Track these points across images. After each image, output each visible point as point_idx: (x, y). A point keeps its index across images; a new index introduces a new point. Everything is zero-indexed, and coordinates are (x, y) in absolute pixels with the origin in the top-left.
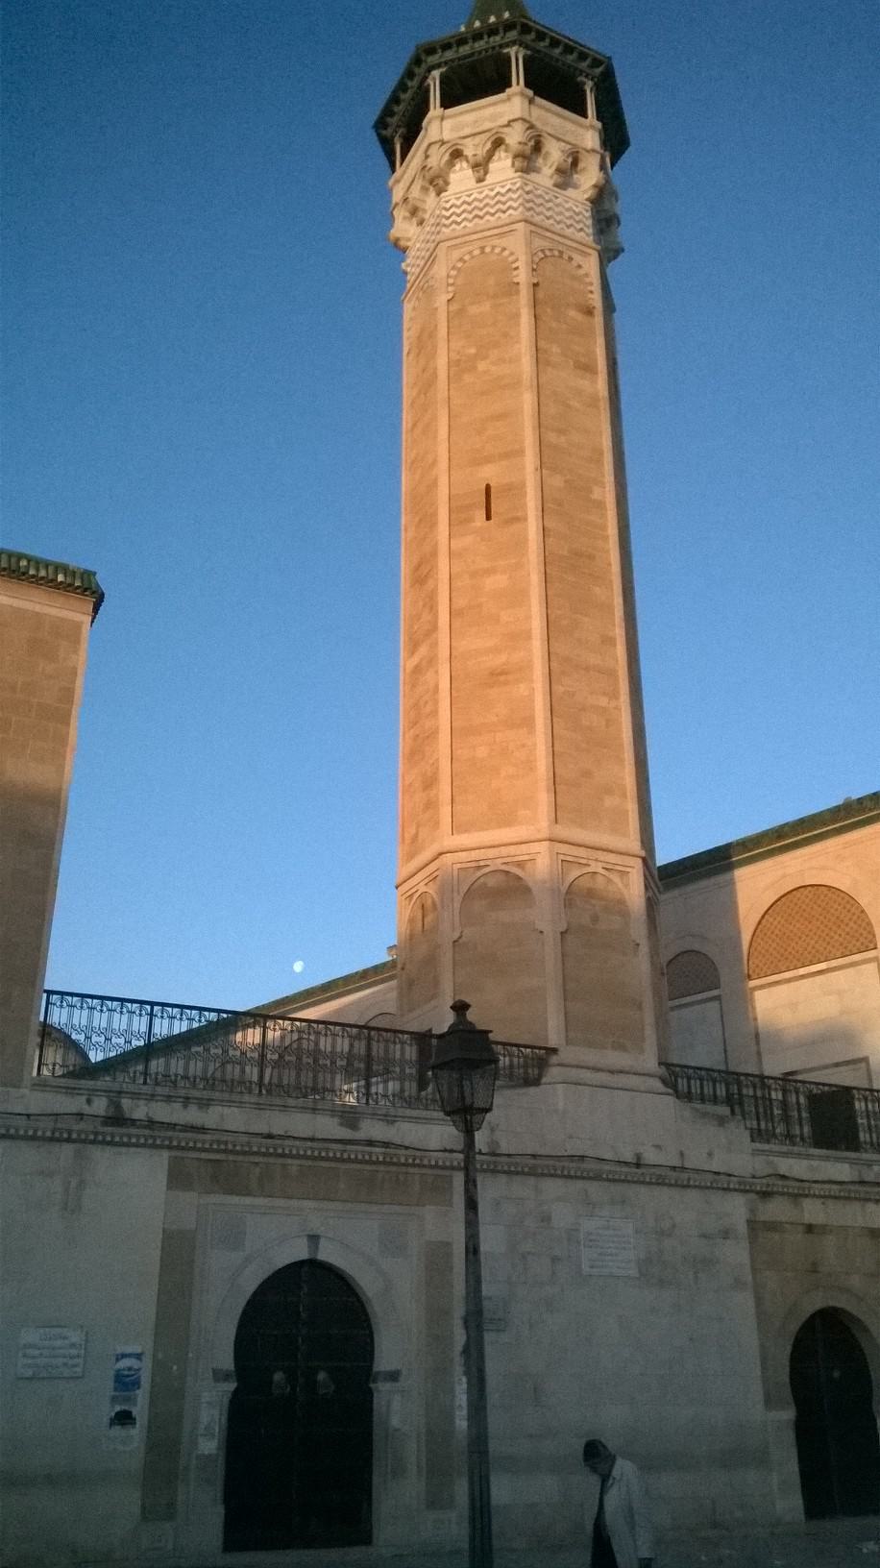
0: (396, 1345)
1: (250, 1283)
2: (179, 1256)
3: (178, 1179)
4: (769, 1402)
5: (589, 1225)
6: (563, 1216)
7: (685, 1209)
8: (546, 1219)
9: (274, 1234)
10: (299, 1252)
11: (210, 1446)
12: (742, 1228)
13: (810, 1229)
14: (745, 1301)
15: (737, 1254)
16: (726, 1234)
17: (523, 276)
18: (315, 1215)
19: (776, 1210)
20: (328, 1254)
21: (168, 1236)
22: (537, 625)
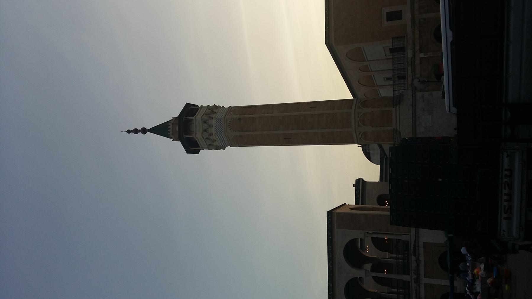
17: (238, 134)
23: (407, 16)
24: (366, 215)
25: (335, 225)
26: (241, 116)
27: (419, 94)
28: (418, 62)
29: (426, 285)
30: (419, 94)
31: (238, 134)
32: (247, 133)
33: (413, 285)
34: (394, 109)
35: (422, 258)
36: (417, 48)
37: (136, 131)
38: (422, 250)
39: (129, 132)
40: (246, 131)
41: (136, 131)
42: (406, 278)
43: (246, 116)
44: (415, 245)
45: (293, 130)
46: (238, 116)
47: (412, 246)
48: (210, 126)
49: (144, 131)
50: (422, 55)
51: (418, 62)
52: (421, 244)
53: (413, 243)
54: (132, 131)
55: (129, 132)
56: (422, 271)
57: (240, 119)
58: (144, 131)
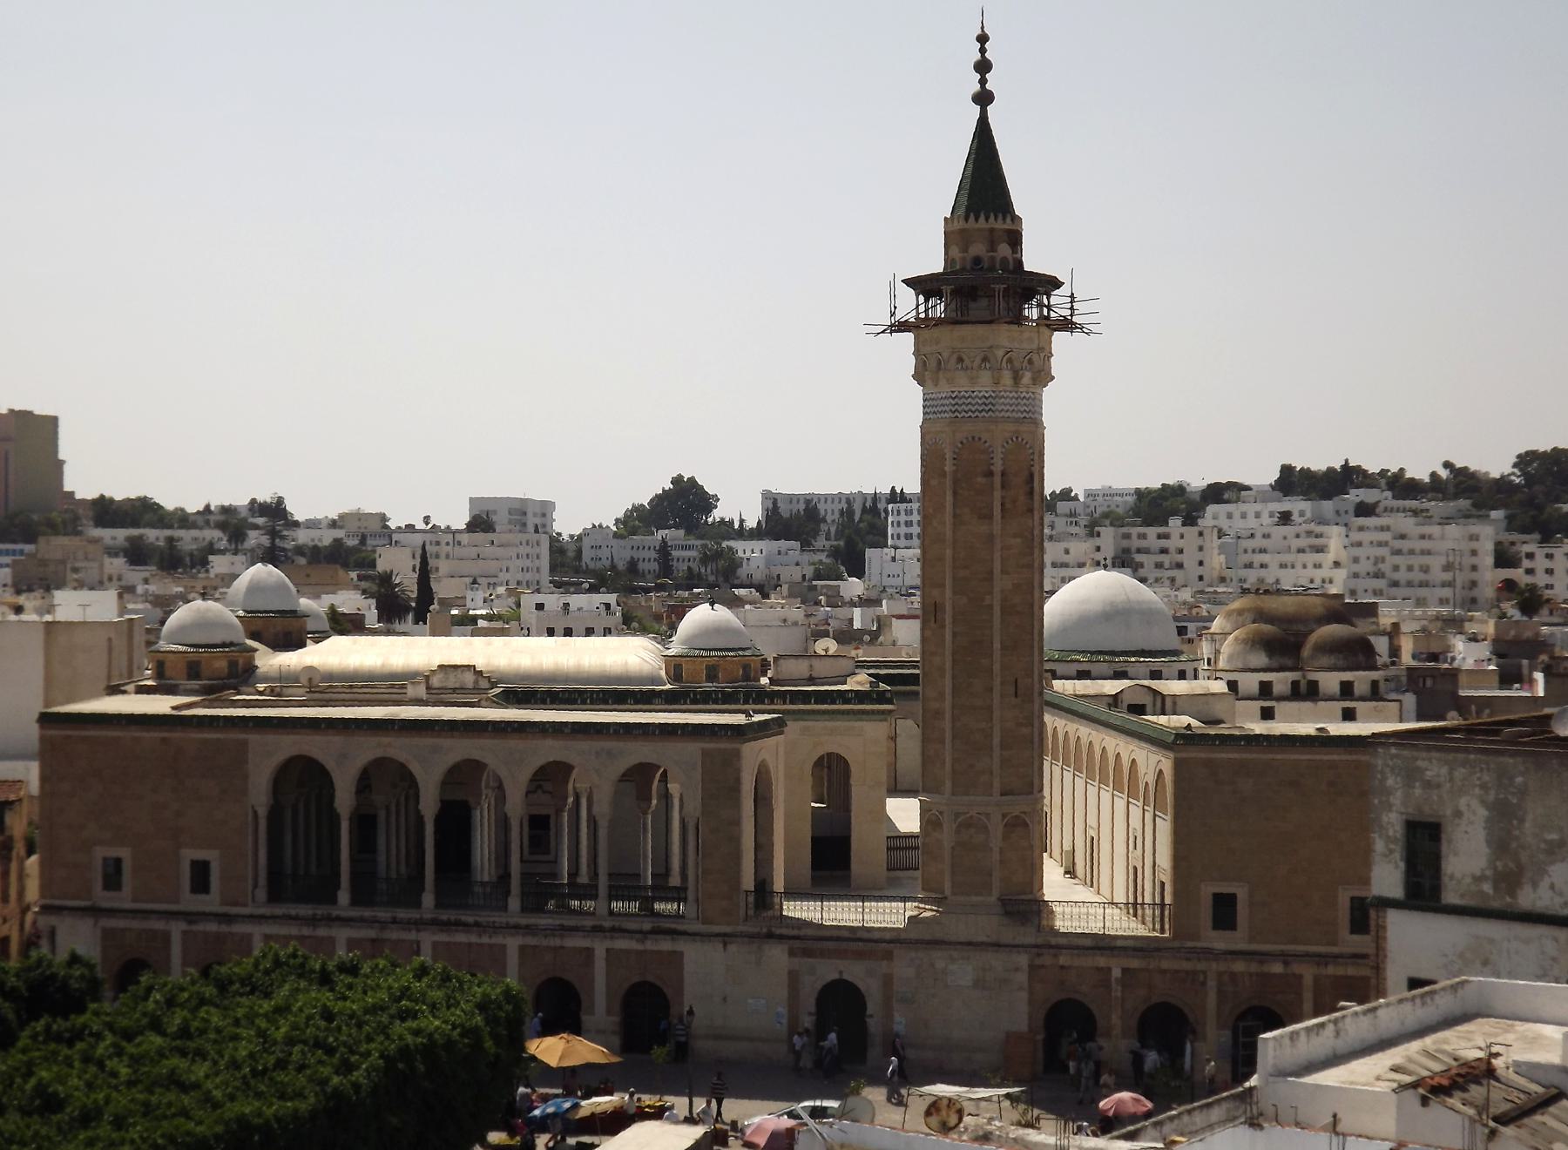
0: (872, 1007)
1: (819, 986)
2: (794, 977)
3: (792, 953)
5: (951, 967)
6: (940, 964)
7: (997, 961)
8: (932, 965)
10: (836, 976)
12: (1025, 967)
13: (1062, 967)
14: (1024, 995)
15: (1022, 978)
16: (1017, 970)
20: (846, 977)
21: (791, 973)
22: (948, 690)
23: (1219, 941)
24: (737, 822)
26: (997, 480)
27: (1023, 960)
28: (1101, 961)
30: (1023, 960)
32: (949, 498)
34: (993, 899)
35: (650, 945)
36: (1135, 963)
37: (983, 67)
38: (665, 945)
39: (983, 39)
40: (955, 493)
41: (983, 67)
43: (998, 494)
45: (954, 635)
46: (998, 467)
47: (673, 926)
49: (984, 98)
51: (1101, 961)
52: (682, 945)
54: (983, 51)
55: (983, 39)
56: (622, 944)
57: (990, 474)
58: (984, 98)
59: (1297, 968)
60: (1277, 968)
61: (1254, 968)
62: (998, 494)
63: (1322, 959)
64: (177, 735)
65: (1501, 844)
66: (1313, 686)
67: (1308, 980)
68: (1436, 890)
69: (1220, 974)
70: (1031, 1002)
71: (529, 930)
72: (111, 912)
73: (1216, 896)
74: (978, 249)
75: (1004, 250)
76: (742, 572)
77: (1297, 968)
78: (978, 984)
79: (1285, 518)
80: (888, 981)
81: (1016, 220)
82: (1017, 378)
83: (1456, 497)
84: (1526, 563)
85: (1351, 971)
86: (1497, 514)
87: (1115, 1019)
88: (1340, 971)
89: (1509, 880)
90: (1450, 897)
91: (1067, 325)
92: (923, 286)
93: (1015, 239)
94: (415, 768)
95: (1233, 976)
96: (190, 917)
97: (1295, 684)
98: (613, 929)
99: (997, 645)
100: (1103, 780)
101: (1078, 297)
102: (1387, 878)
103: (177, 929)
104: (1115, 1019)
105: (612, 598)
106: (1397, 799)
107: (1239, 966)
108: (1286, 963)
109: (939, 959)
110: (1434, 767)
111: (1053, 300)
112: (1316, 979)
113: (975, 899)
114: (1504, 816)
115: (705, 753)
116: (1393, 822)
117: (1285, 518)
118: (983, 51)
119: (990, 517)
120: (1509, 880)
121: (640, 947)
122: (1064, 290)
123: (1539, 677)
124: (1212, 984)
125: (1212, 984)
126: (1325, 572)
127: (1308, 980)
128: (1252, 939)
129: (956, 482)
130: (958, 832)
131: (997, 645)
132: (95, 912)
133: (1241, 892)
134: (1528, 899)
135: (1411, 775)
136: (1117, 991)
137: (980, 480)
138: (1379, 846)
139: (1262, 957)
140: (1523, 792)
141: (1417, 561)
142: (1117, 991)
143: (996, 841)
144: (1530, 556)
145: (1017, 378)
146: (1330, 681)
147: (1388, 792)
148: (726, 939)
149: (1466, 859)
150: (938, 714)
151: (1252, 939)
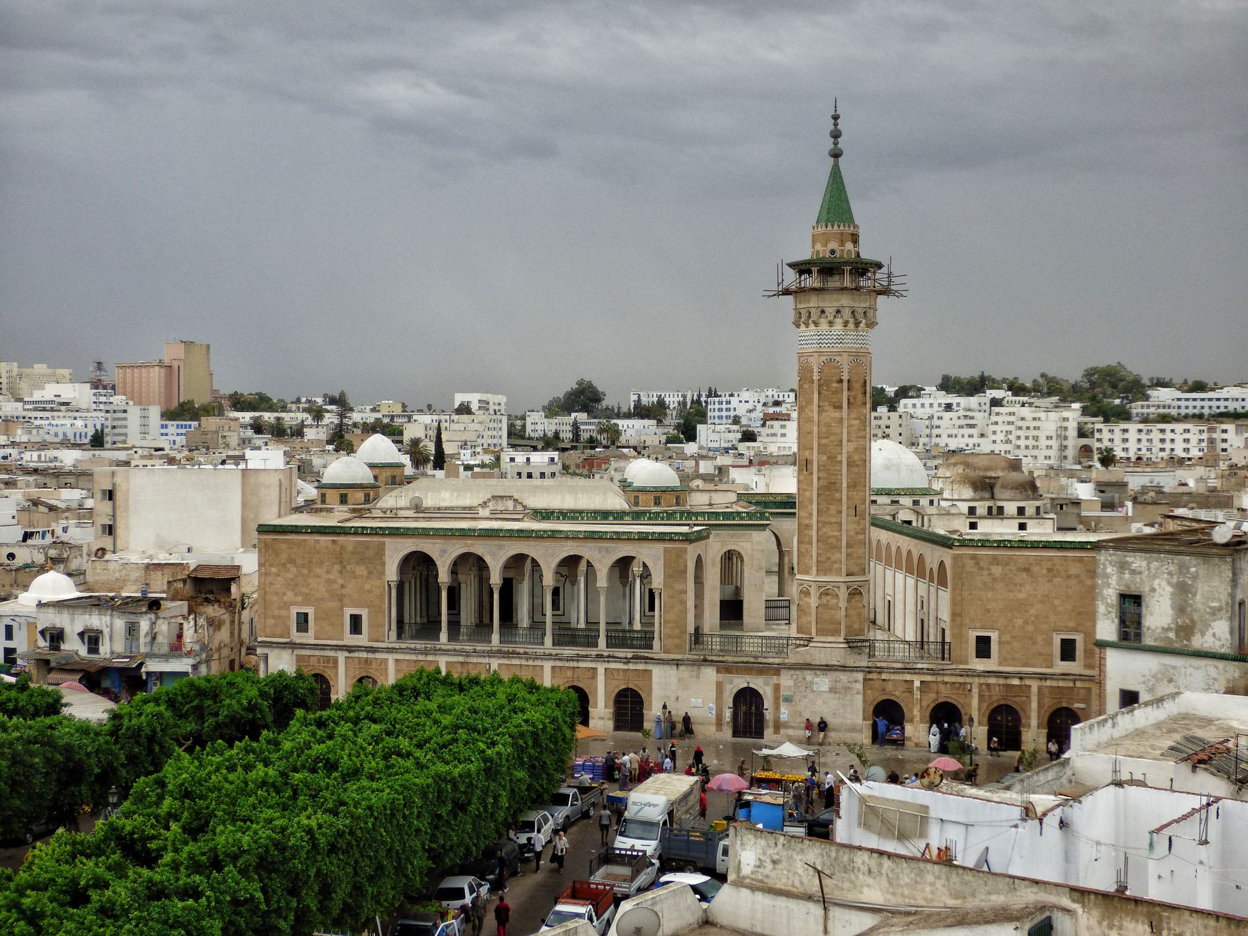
0: (768, 703)
1: (735, 691)
2: (719, 687)
3: (718, 672)
4: (864, 719)
6: (809, 678)
7: (844, 677)
9: (740, 682)
11: (728, 719)
14: (860, 697)
15: (859, 686)
17: (816, 377)
18: (748, 678)
19: (874, 676)
20: (751, 685)
22: (815, 513)
23: (980, 665)
25: (669, 545)
26: (845, 385)
27: (860, 676)
28: (908, 677)
29: (595, 669)
30: (860, 676)
31: (816, 377)
32: (816, 396)
33: (593, 652)
35: (631, 666)
36: (928, 678)
37: (836, 135)
38: (641, 667)
41: (836, 135)
42: (602, 642)
44: (647, 658)
46: (845, 377)
48: (831, 323)
50: (917, 684)
51: (908, 677)
52: (650, 667)
53: (650, 655)
54: (836, 125)
55: (836, 118)
57: (841, 381)
59: (1027, 682)
60: (1016, 682)
61: (1002, 681)
62: (845, 393)
63: (1043, 677)
64: (341, 539)
65: (1181, 609)
66: (1001, 509)
67: (1034, 690)
68: (1138, 636)
69: (981, 685)
70: (864, 701)
71: (557, 658)
72: (303, 646)
73: (978, 638)
74: (833, 245)
75: (849, 246)
76: (623, 440)
77: (1027, 682)
78: (832, 690)
79: (949, 407)
80: (777, 688)
81: (856, 226)
82: (857, 324)
83: (1050, 394)
84: (1097, 435)
85: (1061, 684)
86: (1076, 406)
87: (916, 712)
88: (1054, 684)
89: (1186, 630)
90: (1148, 641)
91: (886, 292)
92: (802, 268)
93: (855, 239)
94: (488, 559)
95: (988, 685)
96: (350, 649)
97: (990, 508)
98: (609, 656)
99: (844, 485)
100: (899, 567)
101: (895, 273)
102: (1107, 629)
103: (341, 656)
104: (916, 712)
105: (555, 455)
106: (1113, 581)
107: (992, 681)
108: (1021, 678)
109: (809, 675)
110: (1138, 561)
111: (878, 276)
112: (1040, 688)
113: (830, 639)
114: (1183, 590)
115: (666, 550)
116: (1110, 594)
117: (949, 407)
118: (836, 125)
119: (841, 407)
120: (1186, 630)
121: (625, 667)
122: (884, 270)
123: (1129, 504)
124: (975, 691)
125: (975, 691)
126: (976, 440)
127: (1034, 690)
128: (1000, 664)
129: (820, 386)
130: (820, 598)
131: (844, 485)
132: (292, 646)
133: (994, 636)
134: (1197, 642)
135: (1123, 567)
136: (917, 695)
137: (835, 385)
138: (1101, 609)
139: (1007, 675)
140: (1195, 577)
141: (1032, 433)
142: (917, 695)
143: (843, 604)
144: (1100, 431)
145: (857, 324)
146: (1011, 508)
147: (1108, 576)
148: (678, 663)
149: (1158, 616)
150: (808, 527)
151: (1000, 664)
